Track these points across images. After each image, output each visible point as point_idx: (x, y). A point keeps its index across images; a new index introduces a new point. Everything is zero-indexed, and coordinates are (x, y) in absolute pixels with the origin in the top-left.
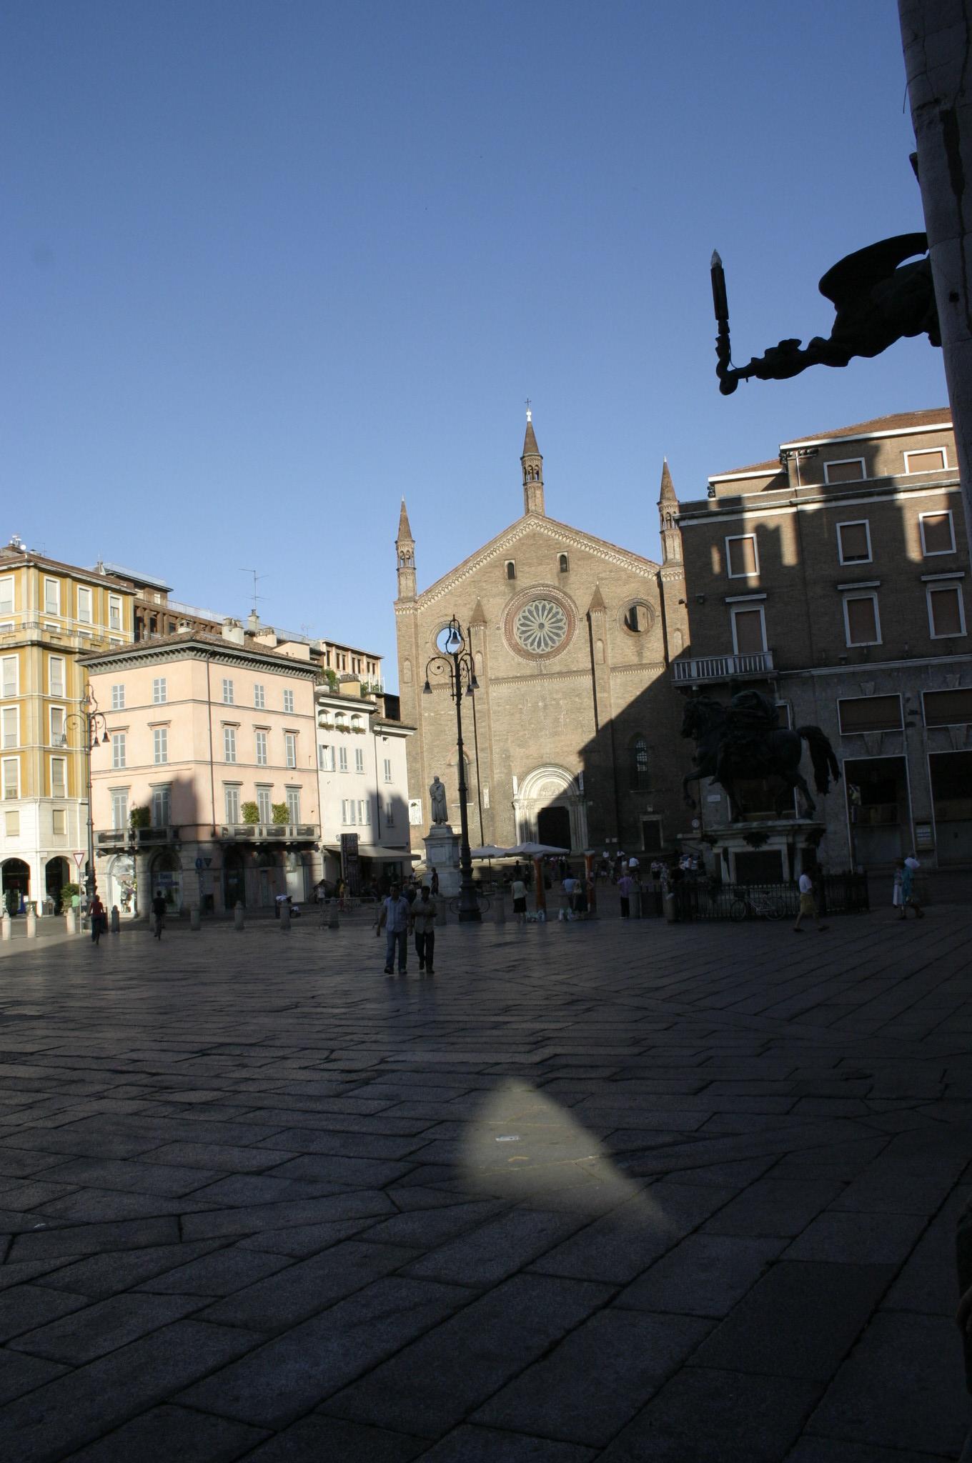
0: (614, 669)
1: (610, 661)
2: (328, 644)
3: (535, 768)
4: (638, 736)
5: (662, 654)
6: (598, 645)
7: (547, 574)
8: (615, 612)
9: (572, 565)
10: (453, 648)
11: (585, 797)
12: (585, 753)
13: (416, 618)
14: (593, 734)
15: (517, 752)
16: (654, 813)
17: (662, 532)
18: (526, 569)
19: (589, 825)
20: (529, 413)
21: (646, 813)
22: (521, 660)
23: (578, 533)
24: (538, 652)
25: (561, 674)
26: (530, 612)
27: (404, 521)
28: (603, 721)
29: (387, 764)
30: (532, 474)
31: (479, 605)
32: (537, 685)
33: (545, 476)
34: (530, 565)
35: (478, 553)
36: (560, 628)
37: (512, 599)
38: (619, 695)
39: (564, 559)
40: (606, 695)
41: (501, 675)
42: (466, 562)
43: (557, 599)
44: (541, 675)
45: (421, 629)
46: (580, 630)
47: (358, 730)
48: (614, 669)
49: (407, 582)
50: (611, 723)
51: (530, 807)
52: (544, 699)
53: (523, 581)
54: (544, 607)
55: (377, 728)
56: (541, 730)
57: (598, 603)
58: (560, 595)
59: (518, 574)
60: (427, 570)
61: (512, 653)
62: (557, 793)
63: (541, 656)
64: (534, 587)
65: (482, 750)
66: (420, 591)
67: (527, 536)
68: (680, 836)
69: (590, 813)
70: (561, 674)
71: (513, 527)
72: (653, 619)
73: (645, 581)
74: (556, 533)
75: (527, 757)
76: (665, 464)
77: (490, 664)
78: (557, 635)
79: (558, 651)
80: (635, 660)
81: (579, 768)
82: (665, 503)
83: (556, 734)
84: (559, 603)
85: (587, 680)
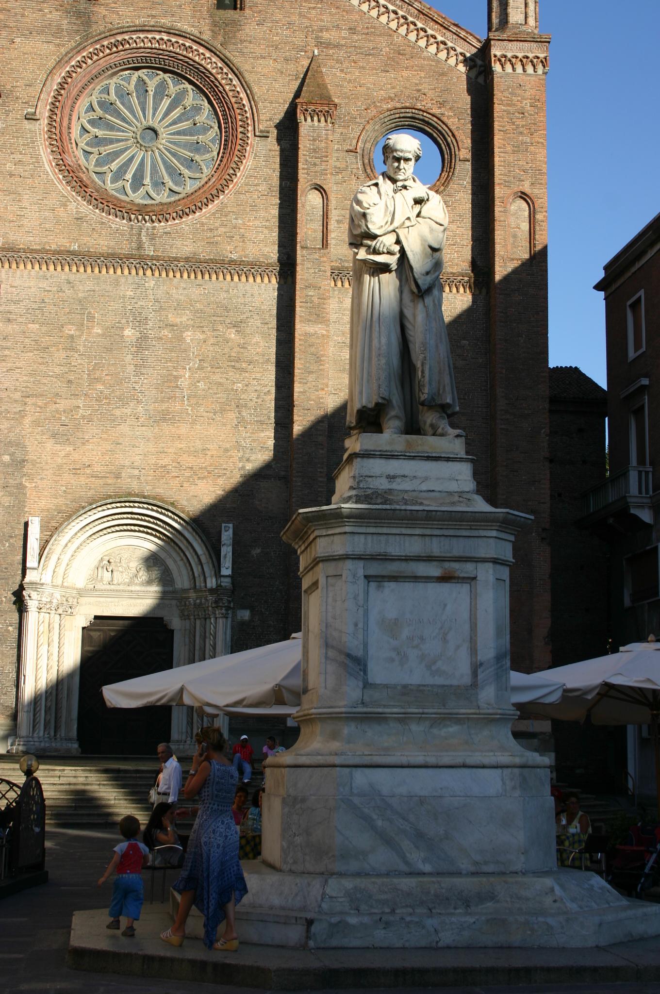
3: (93, 503)
8: (354, 132)
15: (45, 451)
22: (85, 208)
25: (197, 266)
26: (123, 95)
32: (126, 284)
36: (197, 147)
37: (78, 48)
44: (138, 261)
52: (140, 320)
56: (123, 401)
58: (212, 64)
61: (63, 188)
63: (142, 211)
75: (75, 472)
78: (190, 163)
83: (165, 417)
85: (265, 292)
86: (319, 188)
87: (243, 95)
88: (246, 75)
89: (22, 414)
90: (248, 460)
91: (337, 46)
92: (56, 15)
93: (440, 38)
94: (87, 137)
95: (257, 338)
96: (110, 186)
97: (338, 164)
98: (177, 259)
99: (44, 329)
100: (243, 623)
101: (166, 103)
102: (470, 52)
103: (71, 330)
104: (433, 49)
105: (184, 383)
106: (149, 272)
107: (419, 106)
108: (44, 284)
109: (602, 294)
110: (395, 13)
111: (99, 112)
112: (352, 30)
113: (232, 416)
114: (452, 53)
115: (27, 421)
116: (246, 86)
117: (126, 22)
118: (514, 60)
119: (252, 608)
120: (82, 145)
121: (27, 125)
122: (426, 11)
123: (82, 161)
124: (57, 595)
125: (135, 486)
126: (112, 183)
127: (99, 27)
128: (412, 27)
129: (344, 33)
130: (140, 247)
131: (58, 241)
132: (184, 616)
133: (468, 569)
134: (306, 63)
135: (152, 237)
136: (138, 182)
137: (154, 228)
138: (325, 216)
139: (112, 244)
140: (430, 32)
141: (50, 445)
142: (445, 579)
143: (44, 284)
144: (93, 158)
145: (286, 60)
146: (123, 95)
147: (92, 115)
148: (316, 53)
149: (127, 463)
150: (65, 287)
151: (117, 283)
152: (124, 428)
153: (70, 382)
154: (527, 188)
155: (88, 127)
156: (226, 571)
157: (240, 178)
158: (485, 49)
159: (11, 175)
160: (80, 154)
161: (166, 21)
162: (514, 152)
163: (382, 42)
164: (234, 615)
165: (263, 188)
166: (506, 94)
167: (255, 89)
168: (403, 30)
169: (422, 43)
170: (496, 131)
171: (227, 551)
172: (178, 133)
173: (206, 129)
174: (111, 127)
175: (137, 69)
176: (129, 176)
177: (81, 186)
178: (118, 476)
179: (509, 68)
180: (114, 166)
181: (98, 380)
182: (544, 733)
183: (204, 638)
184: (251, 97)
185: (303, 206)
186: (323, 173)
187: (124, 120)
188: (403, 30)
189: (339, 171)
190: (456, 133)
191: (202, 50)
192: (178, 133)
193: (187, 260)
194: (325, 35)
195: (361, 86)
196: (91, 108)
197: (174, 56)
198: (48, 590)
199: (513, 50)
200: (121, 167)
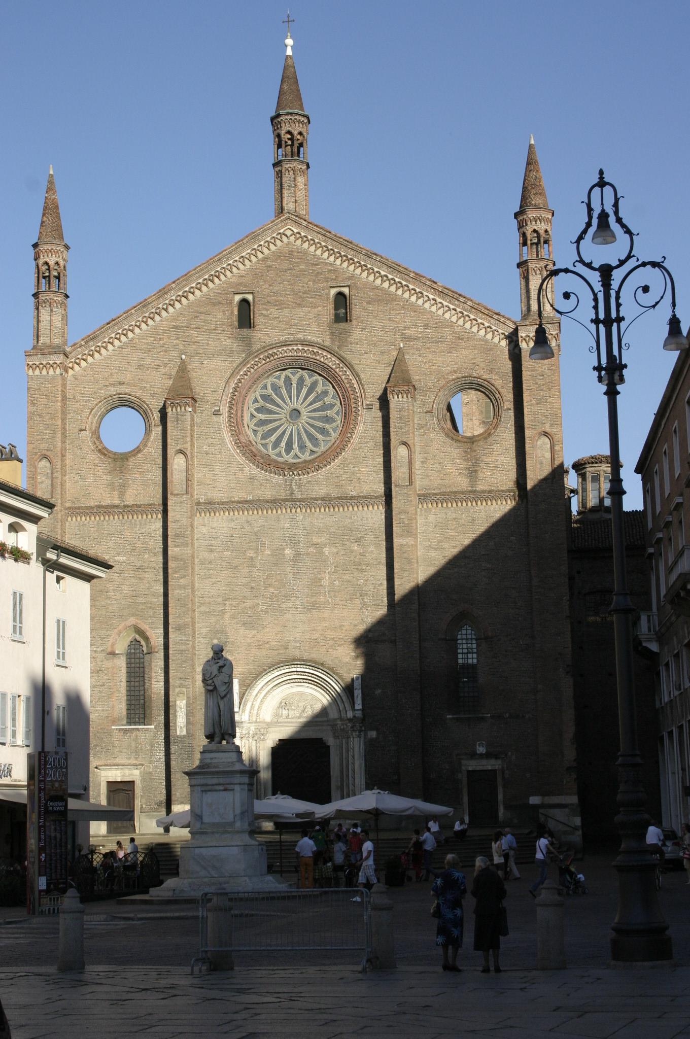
0: (424, 498)
4: (462, 618)
5: (513, 475)
6: (399, 453)
7: (312, 324)
8: (430, 397)
10: (599, 253)
11: (365, 721)
12: (367, 642)
13: (64, 385)
14: (382, 610)
16: (487, 756)
17: (522, 264)
18: (274, 312)
20: (289, 42)
21: (473, 755)
22: (255, 471)
23: (369, 255)
24: (285, 464)
25: (328, 502)
26: (275, 388)
27: (51, 209)
28: (403, 586)
29: (61, 626)
30: (290, 147)
31: (183, 369)
32: (285, 521)
33: (310, 152)
34: (280, 305)
35: (187, 276)
36: (329, 420)
37: (244, 363)
38: (433, 542)
39: (341, 300)
40: (409, 541)
41: (217, 496)
42: (163, 292)
43: (327, 369)
44: (290, 502)
45: (72, 406)
46: (368, 423)
47: (19, 556)
48: (424, 498)
49: (51, 318)
50: (418, 592)
51: (259, 736)
53: (267, 331)
54: (301, 381)
55: (51, 555)
56: (287, 597)
58: (332, 362)
59: (258, 319)
60: (92, 294)
61: (241, 459)
62: (309, 713)
63: (292, 467)
64: (285, 344)
65: (179, 628)
66: (75, 335)
67: (278, 255)
68: (534, 800)
69: (371, 749)
71: (253, 237)
72: (497, 414)
73: (488, 348)
74: (331, 252)
75: (259, 647)
76: (531, 146)
77: (197, 476)
78: (323, 431)
80: (463, 483)
81: (352, 666)
82: (531, 214)
83: (314, 606)
85: (377, 515)
86: (405, 443)
87: (354, 381)
88: (356, 367)
89: (223, 612)
91: (416, 339)
93: (487, 324)
95: (372, 548)
97: (420, 422)
99: (234, 554)
100: (372, 740)
101: (304, 391)
103: (251, 554)
104: (482, 332)
105: (325, 583)
106: (298, 510)
107: (475, 374)
108: (232, 525)
110: (455, 310)
111: (261, 402)
112: (426, 326)
113: (358, 602)
114: (496, 333)
115: (227, 616)
116: (357, 375)
117: (275, 340)
119: (377, 730)
120: (252, 426)
121: (215, 418)
123: (252, 436)
124: (253, 728)
125: (297, 654)
127: (256, 346)
128: (467, 318)
129: (420, 329)
130: (292, 493)
133: (231, 787)
134: (395, 353)
135: (300, 486)
137: (300, 479)
138: (410, 462)
139: (274, 493)
140: (480, 321)
141: (242, 631)
142: (225, 790)
143: (232, 525)
145: (382, 353)
146: (275, 388)
147: (257, 405)
148: (402, 345)
149: (292, 639)
150: (246, 525)
151: (278, 519)
152: (288, 616)
153: (252, 588)
154: (547, 428)
155: (255, 413)
156: (360, 707)
157: (355, 439)
158: (516, 330)
159: (207, 454)
160: (250, 433)
162: (537, 404)
163: (447, 332)
164: (366, 735)
165: (370, 444)
167: (362, 376)
168: (461, 322)
169: (475, 329)
170: (524, 390)
172: (314, 411)
173: (331, 406)
174: (270, 412)
176: (283, 444)
177: (252, 455)
178: (286, 648)
181: (270, 585)
182: (572, 804)
183: (348, 751)
184: (359, 381)
186: (407, 433)
188: (461, 322)
189: (421, 427)
190: (501, 390)
192: (314, 411)
193: (323, 499)
195: (431, 366)
196: (256, 400)
198: (246, 725)
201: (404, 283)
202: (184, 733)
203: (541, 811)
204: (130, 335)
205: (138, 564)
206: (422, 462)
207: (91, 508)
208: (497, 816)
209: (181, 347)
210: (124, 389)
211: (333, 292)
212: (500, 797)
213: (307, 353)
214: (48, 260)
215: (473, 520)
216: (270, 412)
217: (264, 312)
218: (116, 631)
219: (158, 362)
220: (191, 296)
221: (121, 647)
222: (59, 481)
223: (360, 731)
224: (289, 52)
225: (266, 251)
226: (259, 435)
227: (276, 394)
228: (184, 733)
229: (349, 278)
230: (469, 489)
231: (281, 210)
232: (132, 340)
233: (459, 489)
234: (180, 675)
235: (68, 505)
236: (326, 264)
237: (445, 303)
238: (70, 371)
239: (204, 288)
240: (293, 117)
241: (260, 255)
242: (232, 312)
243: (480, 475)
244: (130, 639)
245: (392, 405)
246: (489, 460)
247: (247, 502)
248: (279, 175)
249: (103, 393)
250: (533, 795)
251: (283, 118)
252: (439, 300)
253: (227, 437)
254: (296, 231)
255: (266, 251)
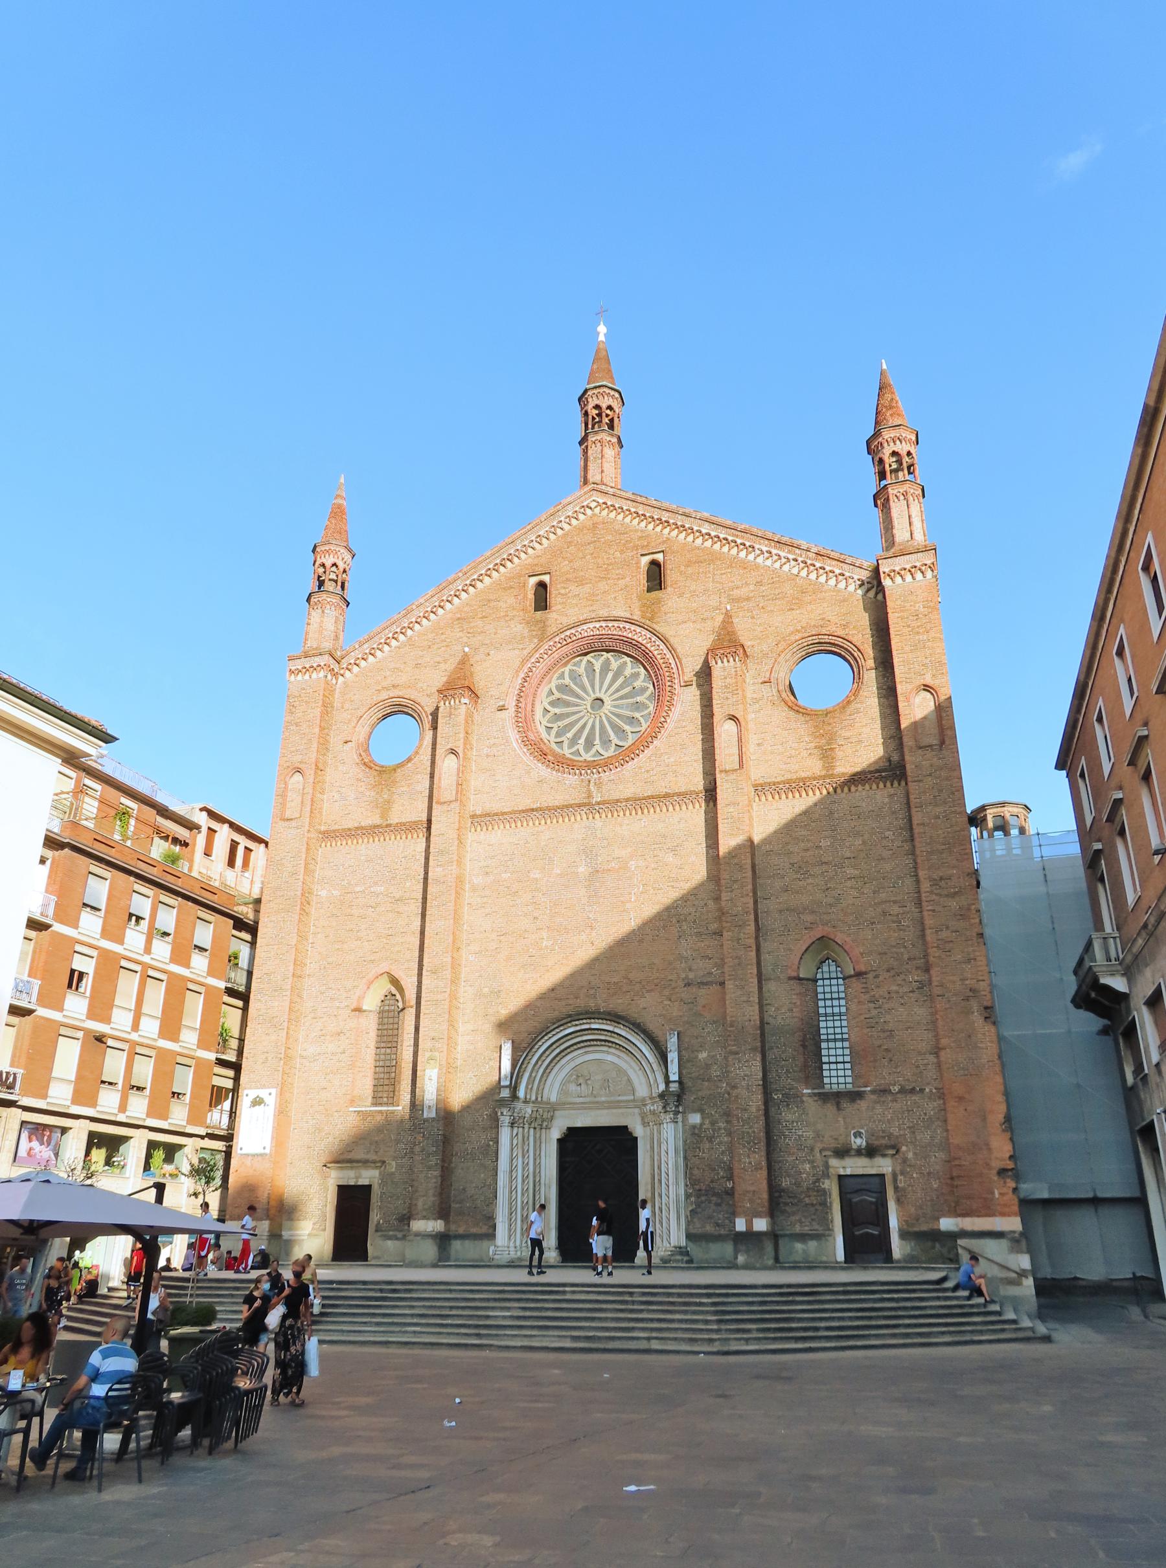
0: (760, 789)
1: (758, 771)
2: (212, 815)
6: (725, 731)
7: (619, 600)
9: (671, 575)
18: (574, 588)
19: (692, 1181)
20: (602, 329)
25: (639, 803)
26: (574, 677)
31: (464, 661)
32: (578, 827)
34: (581, 582)
36: (638, 706)
43: (636, 645)
44: (588, 806)
46: (687, 700)
53: (566, 610)
57: (728, 644)
63: (590, 765)
68: (947, 1224)
69: (694, 1140)
70: (639, 803)
79: (626, 755)
82: (887, 435)
84: (643, 657)
86: (733, 718)
87: (669, 655)
88: (672, 640)
90: (690, 970)
91: (748, 599)
92: (520, 627)
94: (548, 716)
96: (567, 752)
97: (755, 696)
98: (618, 801)
100: (694, 1127)
101: (610, 675)
102: (865, 575)
104: (832, 582)
109: (1064, 773)
111: (557, 695)
114: (851, 581)
116: (671, 649)
117: (573, 620)
118: (903, 572)
119: (701, 1110)
120: (545, 723)
122: (823, 552)
123: (544, 735)
126: (569, 748)
127: (552, 629)
128: (812, 568)
129: (752, 587)
130: (590, 796)
131: (527, 803)
132: (645, 1124)
134: (720, 618)
136: (589, 744)
140: (828, 568)
144: (553, 732)
154: (928, 680)
155: (549, 708)
156: (674, 1077)
157: (670, 724)
159: (488, 756)
161: (604, 613)
166: (899, 602)
167: (679, 650)
169: (823, 579)
171: (673, 1057)
172: (621, 698)
174: (568, 704)
175: (586, 654)
176: (582, 741)
177: (542, 754)
179: (898, 579)
180: (570, 735)
182: (1014, 1232)
185: (720, 736)
187: (578, 696)
189: (756, 701)
190: (861, 648)
191: (633, 627)
194: (736, 593)
195: (768, 628)
196: (551, 693)
197: (611, 638)
199: (899, 563)
200: (575, 735)
201: (730, 538)
202: (433, 1115)
203: (959, 1242)
204: (409, 632)
205: (398, 896)
206: (759, 745)
207: (349, 829)
208: (889, 1251)
209: (465, 639)
210: (397, 693)
211: (645, 560)
212: (893, 1222)
213: (613, 629)
214: (324, 560)
215: (831, 813)
216: (568, 704)
217: (563, 591)
218: (364, 980)
219: (438, 659)
220: (479, 584)
221: (372, 1002)
222: (309, 797)
223: (677, 1113)
224: (602, 338)
225: (566, 527)
226: (553, 732)
227: (576, 684)
228: (433, 1115)
229: (664, 542)
230: (823, 773)
231: (586, 482)
232: (410, 638)
233: (809, 774)
234: (433, 1034)
235: (323, 828)
236: (636, 531)
237: (782, 554)
238: (341, 679)
239: (495, 574)
240: (601, 390)
241: (559, 532)
242: (525, 596)
243: (839, 753)
244: (384, 992)
245: (717, 683)
246: (848, 734)
247: (533, 810)
248: (585, 452)
249: (376, 699)
250: (944, 1216)
251: (590, 393)
252: (774, 551)
253: (513, 735)
254: (601, 501)
255: (566, 527)
